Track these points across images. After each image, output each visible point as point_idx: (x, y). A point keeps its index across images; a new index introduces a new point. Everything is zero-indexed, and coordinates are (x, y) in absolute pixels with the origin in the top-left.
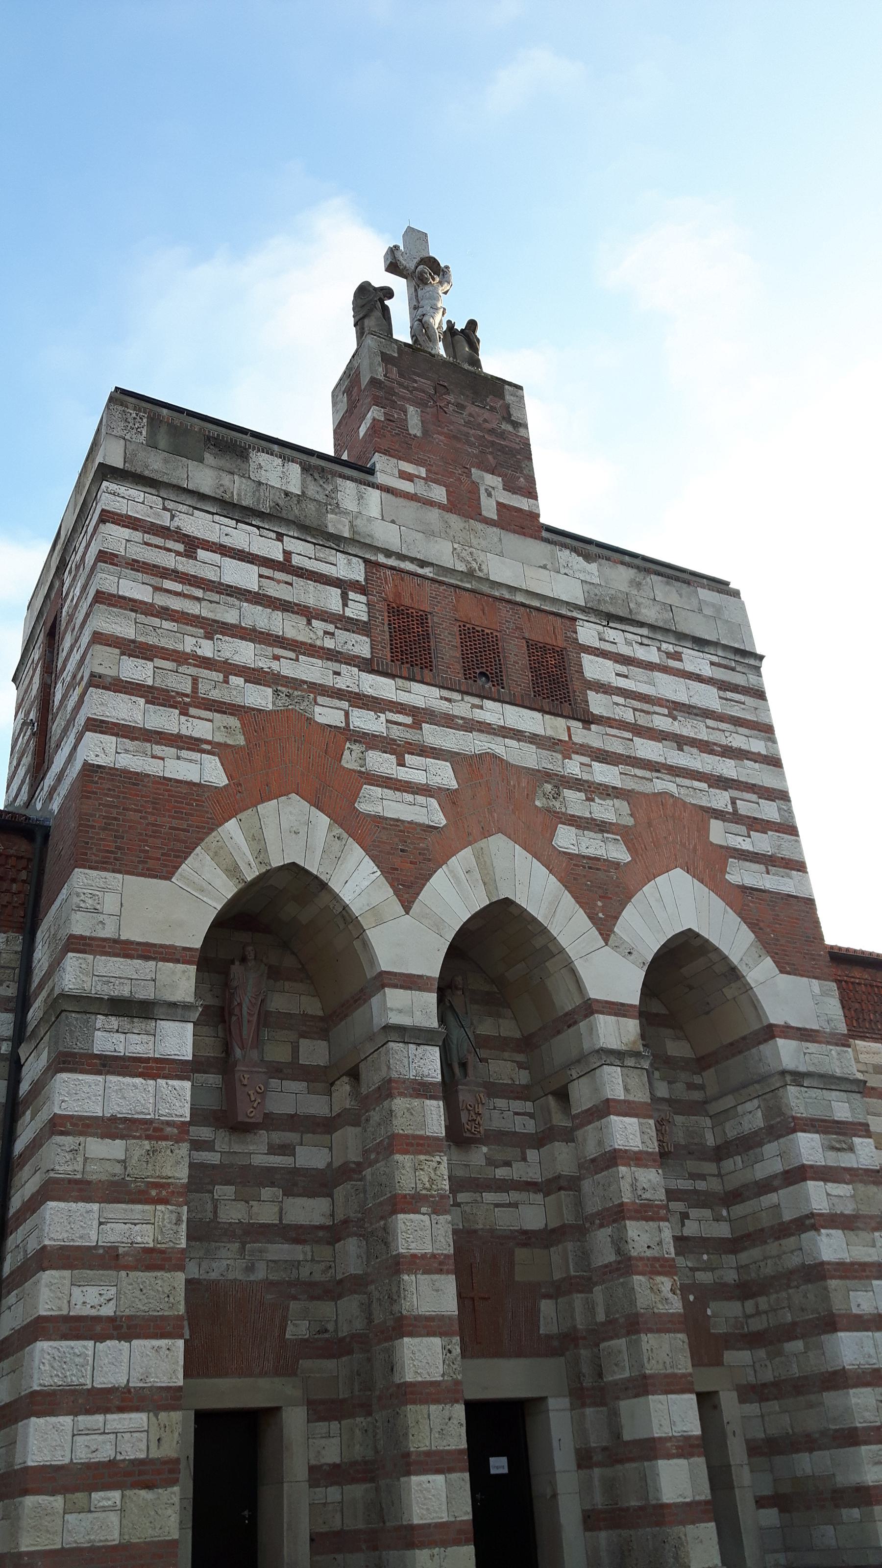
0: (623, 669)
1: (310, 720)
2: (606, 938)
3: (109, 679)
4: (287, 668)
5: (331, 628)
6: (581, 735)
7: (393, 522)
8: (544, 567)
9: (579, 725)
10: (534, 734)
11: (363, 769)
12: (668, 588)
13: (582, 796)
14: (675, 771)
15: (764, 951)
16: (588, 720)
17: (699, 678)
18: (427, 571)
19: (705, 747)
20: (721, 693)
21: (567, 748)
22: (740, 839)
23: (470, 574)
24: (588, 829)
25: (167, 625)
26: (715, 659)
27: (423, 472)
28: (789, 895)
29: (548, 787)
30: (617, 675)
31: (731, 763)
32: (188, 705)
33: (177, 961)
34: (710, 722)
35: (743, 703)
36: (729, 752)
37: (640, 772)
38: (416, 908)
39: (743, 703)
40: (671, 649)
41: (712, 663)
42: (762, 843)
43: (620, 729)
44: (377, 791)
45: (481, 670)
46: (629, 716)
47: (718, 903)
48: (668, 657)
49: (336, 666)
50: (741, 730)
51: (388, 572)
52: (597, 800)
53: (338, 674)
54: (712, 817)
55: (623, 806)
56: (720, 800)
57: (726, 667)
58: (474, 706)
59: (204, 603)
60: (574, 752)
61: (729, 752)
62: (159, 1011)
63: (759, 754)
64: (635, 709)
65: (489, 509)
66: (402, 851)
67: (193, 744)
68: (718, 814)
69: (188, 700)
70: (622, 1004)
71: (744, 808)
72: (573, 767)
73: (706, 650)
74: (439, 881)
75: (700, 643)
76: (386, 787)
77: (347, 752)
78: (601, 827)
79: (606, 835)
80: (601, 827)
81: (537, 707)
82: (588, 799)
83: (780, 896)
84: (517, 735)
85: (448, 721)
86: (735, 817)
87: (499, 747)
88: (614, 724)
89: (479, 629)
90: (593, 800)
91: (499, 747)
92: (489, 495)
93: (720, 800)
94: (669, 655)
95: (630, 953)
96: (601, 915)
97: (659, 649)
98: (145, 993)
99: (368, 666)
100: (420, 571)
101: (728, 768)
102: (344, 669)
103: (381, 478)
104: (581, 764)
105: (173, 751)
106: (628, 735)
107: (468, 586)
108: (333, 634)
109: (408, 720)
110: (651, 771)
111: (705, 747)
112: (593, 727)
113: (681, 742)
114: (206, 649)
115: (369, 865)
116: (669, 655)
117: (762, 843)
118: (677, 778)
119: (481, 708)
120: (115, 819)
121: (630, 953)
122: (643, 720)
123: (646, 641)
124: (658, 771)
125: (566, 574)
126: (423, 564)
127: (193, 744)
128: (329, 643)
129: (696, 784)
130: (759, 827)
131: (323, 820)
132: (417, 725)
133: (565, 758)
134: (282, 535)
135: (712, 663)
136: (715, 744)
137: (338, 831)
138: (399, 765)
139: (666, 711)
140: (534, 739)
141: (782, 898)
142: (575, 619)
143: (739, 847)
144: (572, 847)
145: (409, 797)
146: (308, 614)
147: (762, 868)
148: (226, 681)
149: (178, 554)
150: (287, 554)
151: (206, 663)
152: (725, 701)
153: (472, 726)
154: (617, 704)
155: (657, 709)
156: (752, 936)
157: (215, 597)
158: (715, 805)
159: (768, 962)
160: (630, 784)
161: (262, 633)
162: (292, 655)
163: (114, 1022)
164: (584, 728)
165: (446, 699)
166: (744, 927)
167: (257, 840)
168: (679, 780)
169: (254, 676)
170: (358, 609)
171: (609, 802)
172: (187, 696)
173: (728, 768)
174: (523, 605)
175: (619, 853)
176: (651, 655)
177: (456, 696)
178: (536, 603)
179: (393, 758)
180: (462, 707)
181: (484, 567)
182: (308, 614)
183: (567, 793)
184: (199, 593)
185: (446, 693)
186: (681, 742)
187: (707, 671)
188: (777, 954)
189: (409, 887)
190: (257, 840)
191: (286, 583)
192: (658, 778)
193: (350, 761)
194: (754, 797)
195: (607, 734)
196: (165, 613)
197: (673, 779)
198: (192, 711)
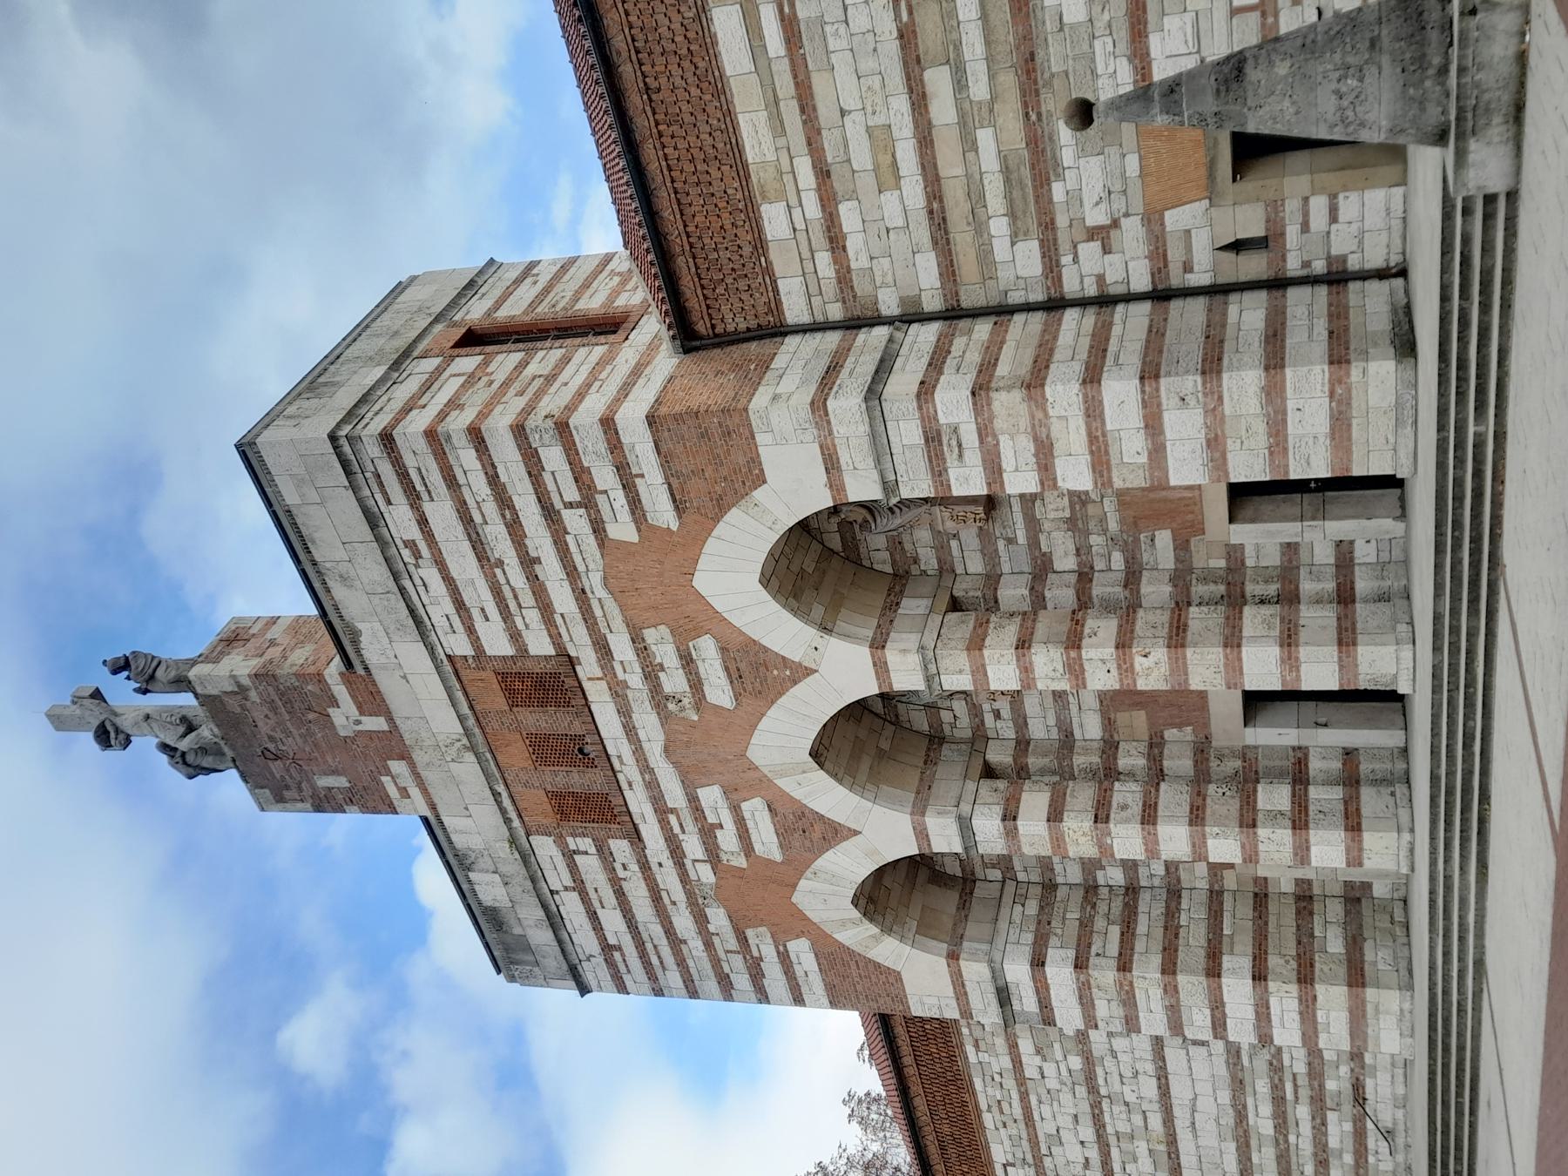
0: (476, 613)
1: (718, 886)
2: (809, 672)
3: (759, 996)
4: (678, 893)
5: (618, 866)
6: (588, 667)
7: (467, 809)
8: (404, 677)
9: (578, 668)
10: (619, 713)
11: (742, 854)
12: (316, 535)
13: (661, 675)
14: (572, 573)
15: (747, 498)
17: (423, 522)
18: (501, 788)
20: (425, 496)
22: (616, 505)
23: (472, 748)
24: (697, 674)
25: (691, 963)
26: (379, 497)
27: (385, 779)
28: (659, 453)
29: (671, 706)
30: (487, 620)
31: (518, 502)
32: (752, 957)
33: (959, 970)
34: (478, 519)
35: (419, 469)
37: (598, 612)
38: (853, 826)
39: (419, 469)
40: (406, 553)
41: (389, 502)
42: (605, 476)
43: (556, 626)
44: (758, 848)
45: (577, 752)
46: (533, 616)
47: (711, 545)
48: (421, 557)
49: (655, 867)
50: (461, 480)
51: (526, 819)
52: (658, 660)
53: (660, 865)
54: (606, 536)
55: (650, 635)
56: (576, 521)
57: (381, 485)
58: (622, 763)
59: (656, 942)
60: (616, 677)
62: (1001, 983)
63: (480, 459)
64: (520, 606)
66: (804, 832)
68: (598, 528)
69: (748, 957)
70: (875, 665)
71: (572, 494)
72: (635, 680)
73: (376, 509)
75: (373, 520)
76: (750, 838)
77: (732, 863)
79: (694, 657)
80: (687, 661)
81: (587, 710)
82: (663, 669)
83: (666, 465)
84: (630, 731)
85: (653, 786)
87: (655, 752)
88: (554, 632)
89: (531, 749)
90: (661, 665)
91: (655, 752)
92: (358, 722)
93: (576, 521)
94: (417, 555)
95: (816, 649)
96: (788, 673)
97: (417, 566)
98: (990, 989)
99: (635, 837)
100: (505, 795)
102: (653, 862)
104: (625, 672)
105: (796, 967)
106: (559, 620)
107: (488, 756)
108: (623, 865)
109: (673, 819)
110: (588, 599)
112: (573, 653)
113: (529, 563)
115: (829, 855)
116: (417, 555)
117: (605, 476)
118: (579, 569)
119: (619, 757)
120: (866, 996)
121: (816, 649)
122: (527, 599)
123: (418, 582)
124: (583, 591)
125: (396, 657)
126: (496, 795)
128: (634, 867)
129: (573, 547)
130: (585, 477)
131: (803, 884)
132: (672, 811)
133: (628, 687)
134: (551, 891)
135: (389, 502)
136: (503, 516)
137: (808, 873)
138: (721, 826)
139: (498, 571)
140: (625, 712)
141: (667, 462)
142: (449, 657)
143: (626, 507)
144: (726, 692)
145: (750, 824)
147: (638, 481)
148: (718, 934)
149: (623, 955)
150: (566, 888)
151: (709, 945)
152: (433, 495)
153: (645, 768)
154: (527, 626)
155: (502, 580)
156: (734, 510)
157: (645, 936)
158: (588, 529)
159: (759, 494)
160: (618, 622)
161: (657, 911)
162: (664, 894)
163: (1015, 1002)
164: (580, 664)
165: (630, 785)
166: (727, 518)
167: (843, 923)
168: (581, 568)
171: (654, 648)
172: (745, 958)
174: (471, 707)
176: (431, 574)
177: (621, 777)
178: (459, 695)
179: (719, 833)
180: (629, 771)
181: (455, 737)
183: (668, 688)
184: (649, 946)
185: (624, 785)
186: (529, 563)
188: (744, 483)
189: (836, 830)
190: (843, 923)
191: (596, 891)
192: (593, 593)
193: (741, 862)
194: (547, 477)
195: (572, 640)
196: (681, 963)
197: (583, 576)
198: (756, 954)
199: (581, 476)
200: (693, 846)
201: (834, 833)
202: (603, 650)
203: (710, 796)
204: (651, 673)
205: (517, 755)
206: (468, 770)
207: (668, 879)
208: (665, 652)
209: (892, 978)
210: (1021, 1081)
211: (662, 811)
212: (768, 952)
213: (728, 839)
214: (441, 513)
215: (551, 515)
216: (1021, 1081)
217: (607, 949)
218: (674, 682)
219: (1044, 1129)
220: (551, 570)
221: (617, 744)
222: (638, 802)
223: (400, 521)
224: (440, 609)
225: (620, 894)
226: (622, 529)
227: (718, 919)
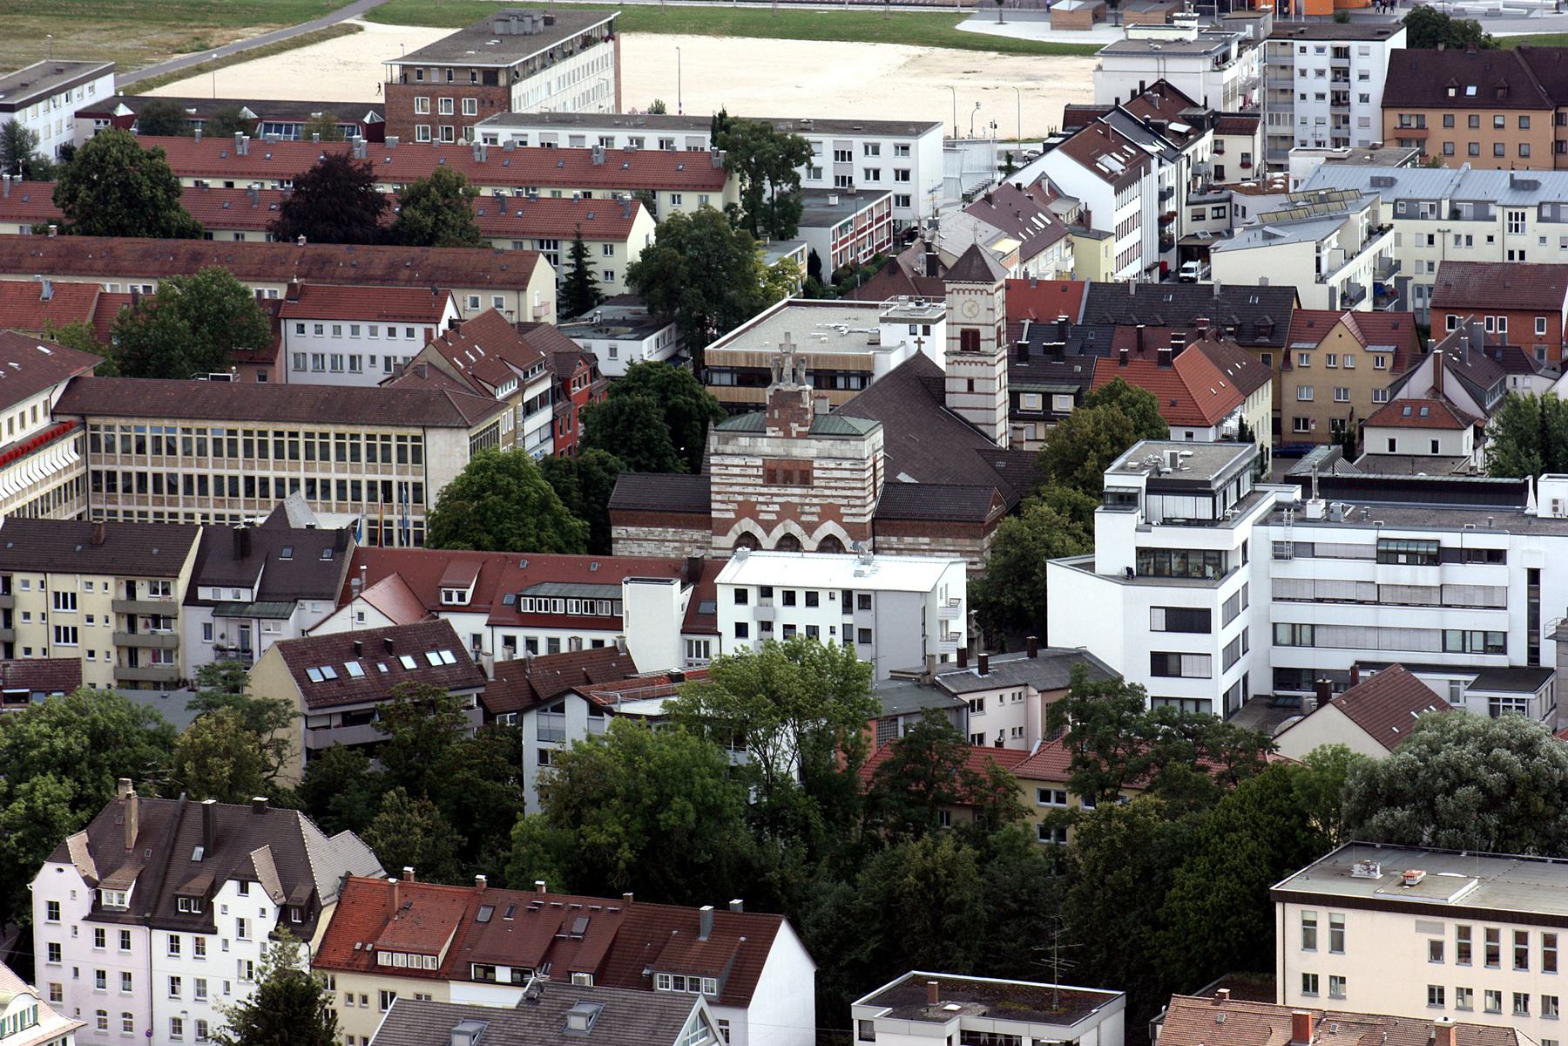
16: (812, 488)
19: (844, 488)
21: (805, 496)
36: (850, 489)
42: (854, 511)
56: (845, 502)
61: (850, 489)
65: (794, 434)
67: (728, 510)
72: (807, 501)
74: (775, 530)
78: (812, 513)
80: (812, 513)
86: (849, 505)
87: (789, 499)
91: (789, 499)
93: (845, 502)
99: (762, 486)
101: (849, 493)
103: (769, 434)
111: (844, 488)
113: (836, 488)
114: (731, 490)
117: (854, 511)
127: (728, 510)
140: (801, 496)
146: (750, 476)
153: (784, 495)
169: (739, 494)
170: (761, 473)
173: (849, 493)
175: (815, 519)
176: (833, 466)
180: (782, 491)
182: (750, 476)
186: (836, 488)
187: (848, 466)
199: (855, 506)
200: (761, 499)
201: (768, 531)
202: (816, 496)
203: (777, 508)
204: (811, 505)
205: (787, 467)
206: (781, 451)
207: (750, 490)
208: (814, 509)
209: (725, 534)
210: (663, 541)
211: (773, 495)
212: (730, 507)
213: (764, 508)
214: (847, 474)
215: (847, 497)
216: (663, 541)
217: (727, 466)
218: (807, 509)
219: (645, 544)
220: (834, 493)
221: (789, 491)
222: (774, 490)
223: (846, 464)
224: (826, 464)
225: (745, 476)
226: (843, 510)
227: (740, 498)
